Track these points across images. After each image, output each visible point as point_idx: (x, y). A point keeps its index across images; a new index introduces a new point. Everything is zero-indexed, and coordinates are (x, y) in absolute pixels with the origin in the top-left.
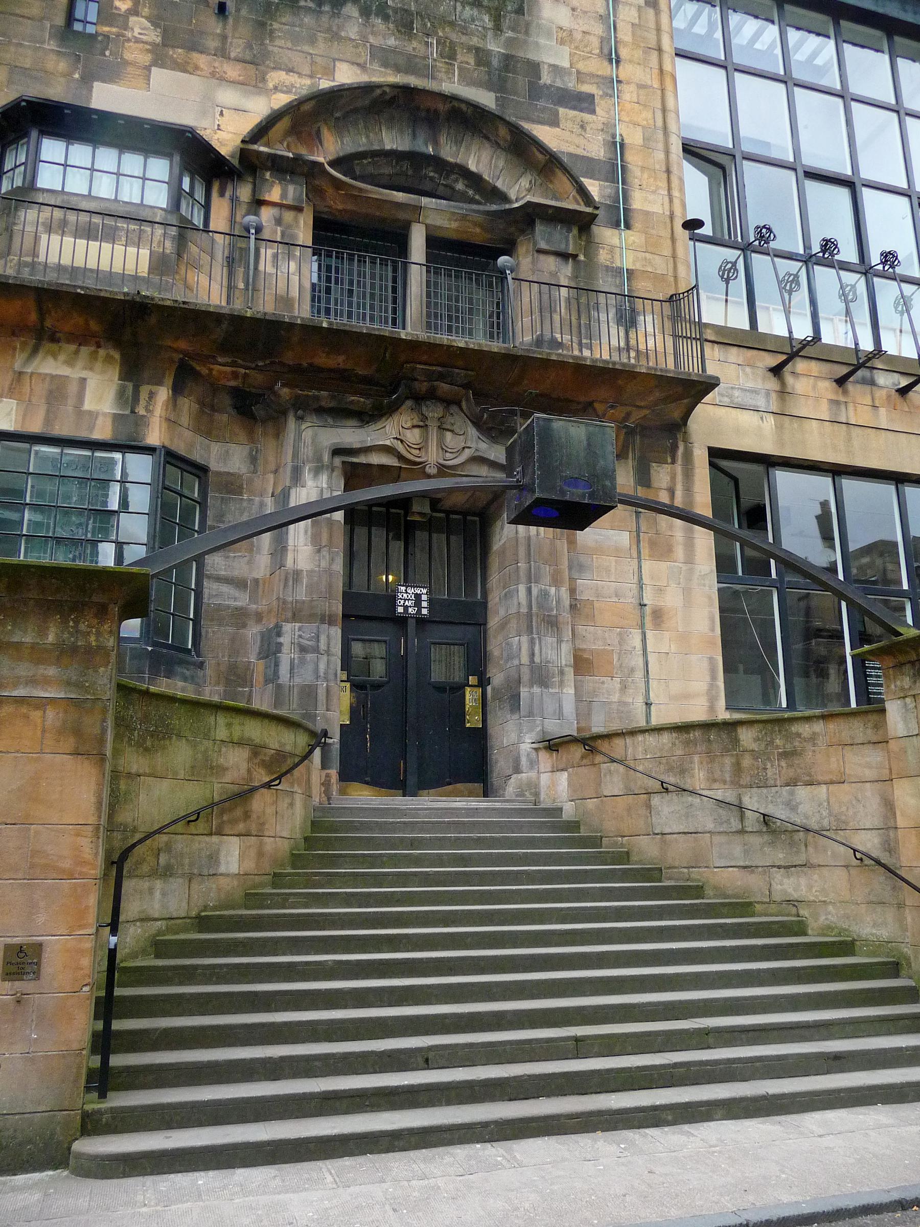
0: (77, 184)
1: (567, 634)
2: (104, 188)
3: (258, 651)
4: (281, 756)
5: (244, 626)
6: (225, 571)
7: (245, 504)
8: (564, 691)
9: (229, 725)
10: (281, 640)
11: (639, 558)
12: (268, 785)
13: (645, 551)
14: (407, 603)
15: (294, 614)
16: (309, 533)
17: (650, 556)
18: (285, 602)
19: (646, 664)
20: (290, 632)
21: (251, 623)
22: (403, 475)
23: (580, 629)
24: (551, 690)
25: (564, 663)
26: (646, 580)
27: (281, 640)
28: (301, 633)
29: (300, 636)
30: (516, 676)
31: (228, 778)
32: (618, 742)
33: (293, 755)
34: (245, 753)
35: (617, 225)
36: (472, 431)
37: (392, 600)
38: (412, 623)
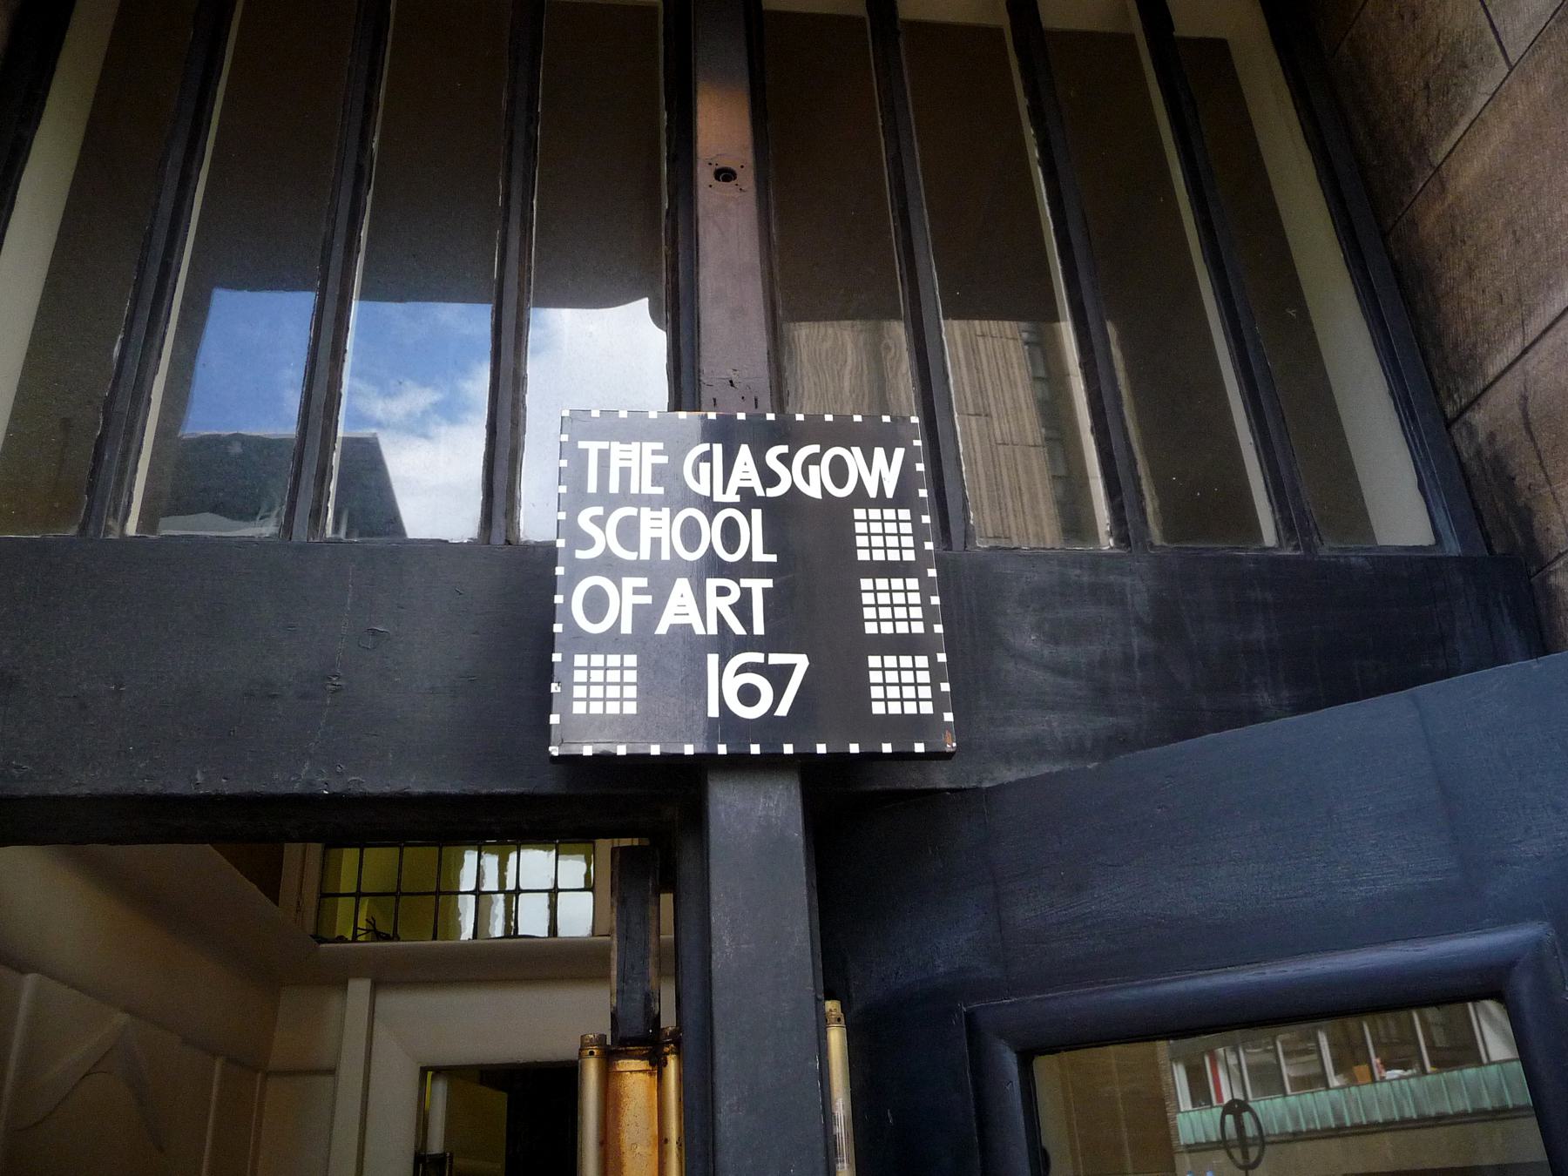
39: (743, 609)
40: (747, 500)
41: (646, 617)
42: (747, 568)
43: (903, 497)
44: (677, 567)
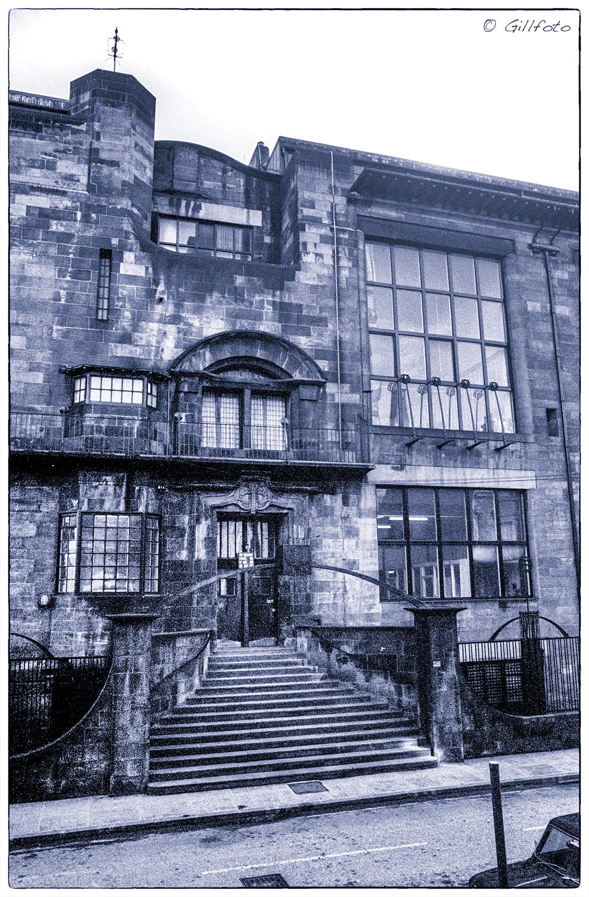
0: (106, 398)
2: (116, 398)
35: (337, 382)
36: (270, 493)
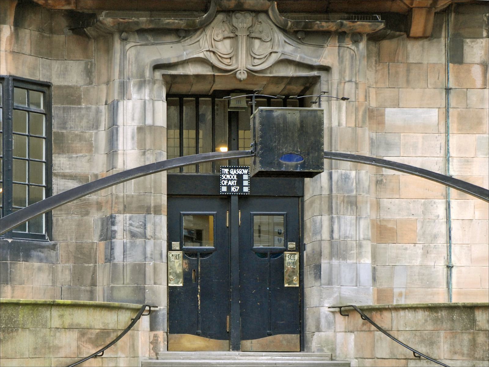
1: (367, 211)
3: (99, 234)
4: (105, 332)
5: (87, 214)
6: (70, 169)
7: (83, 112)
8: (362, 261)
9: (61, 316)
10: (115, 228)
11: (447, 133)
12: (95, 356)
13: (453, 126)
14: (230, 183)
15: (125, 206)
16: (136, 139)
17: (459, 130)
18: (117, 197)
19: (449, 230)
20: (122, 222)
21: (93, 210)
22: (217, 79)
23: (385, 202)
24: (349, 261)
25: (362, 237)
26: (453, 153)
27: (115, 228)
28: (131, 222)
29: (131, 225)
30: (318, 250)
31: (62, 353)
32: (386, 314)
33: (115, 330)
34: (75, 335)
37: (217, 180)
38: (235, 200)
39: (234, 183)
40: (235, 174)
41: (227, 184)
42: (235, 180)
43: (248, 174)
44: (229, 180)
